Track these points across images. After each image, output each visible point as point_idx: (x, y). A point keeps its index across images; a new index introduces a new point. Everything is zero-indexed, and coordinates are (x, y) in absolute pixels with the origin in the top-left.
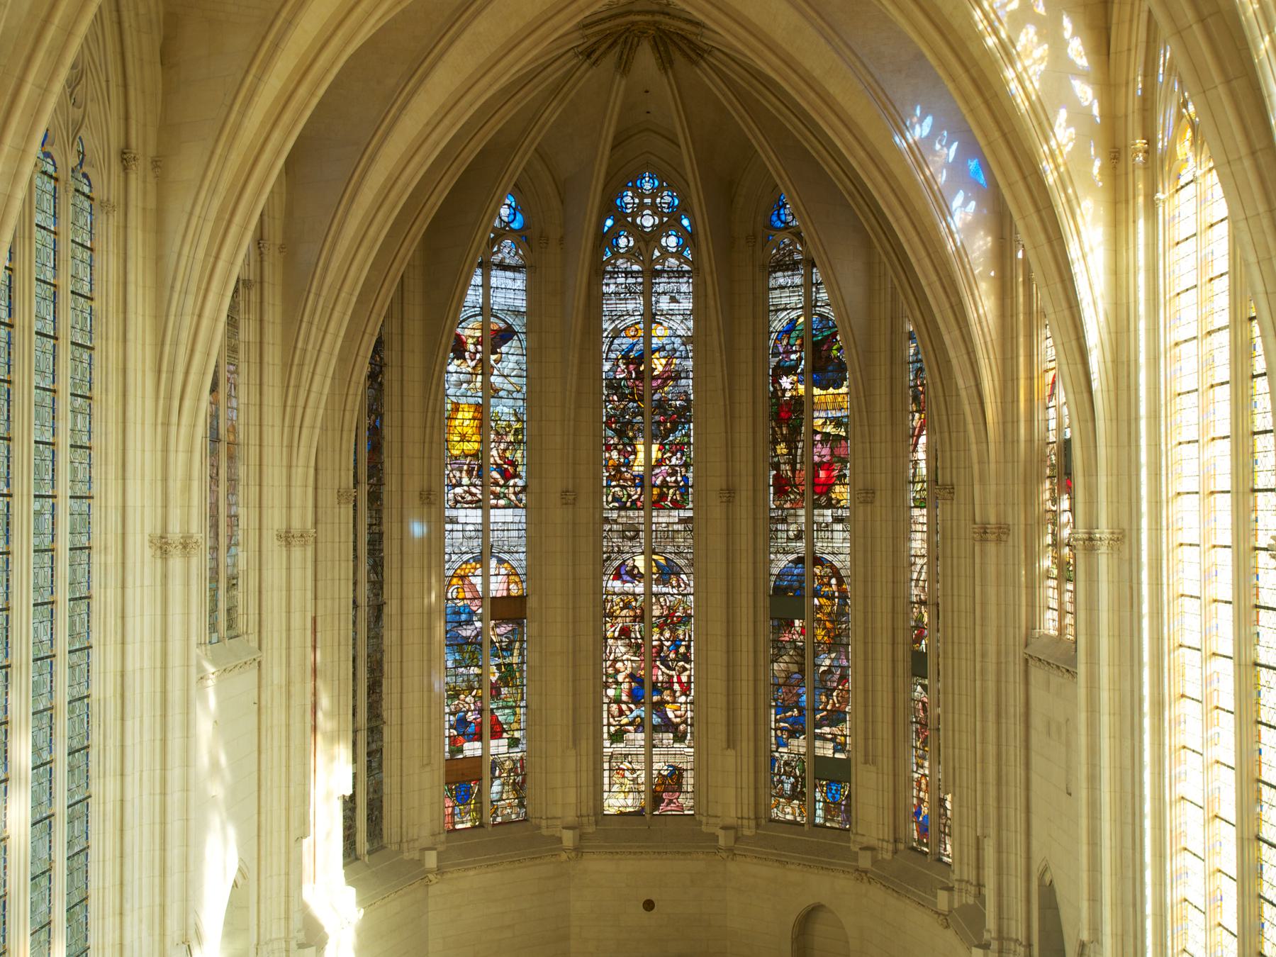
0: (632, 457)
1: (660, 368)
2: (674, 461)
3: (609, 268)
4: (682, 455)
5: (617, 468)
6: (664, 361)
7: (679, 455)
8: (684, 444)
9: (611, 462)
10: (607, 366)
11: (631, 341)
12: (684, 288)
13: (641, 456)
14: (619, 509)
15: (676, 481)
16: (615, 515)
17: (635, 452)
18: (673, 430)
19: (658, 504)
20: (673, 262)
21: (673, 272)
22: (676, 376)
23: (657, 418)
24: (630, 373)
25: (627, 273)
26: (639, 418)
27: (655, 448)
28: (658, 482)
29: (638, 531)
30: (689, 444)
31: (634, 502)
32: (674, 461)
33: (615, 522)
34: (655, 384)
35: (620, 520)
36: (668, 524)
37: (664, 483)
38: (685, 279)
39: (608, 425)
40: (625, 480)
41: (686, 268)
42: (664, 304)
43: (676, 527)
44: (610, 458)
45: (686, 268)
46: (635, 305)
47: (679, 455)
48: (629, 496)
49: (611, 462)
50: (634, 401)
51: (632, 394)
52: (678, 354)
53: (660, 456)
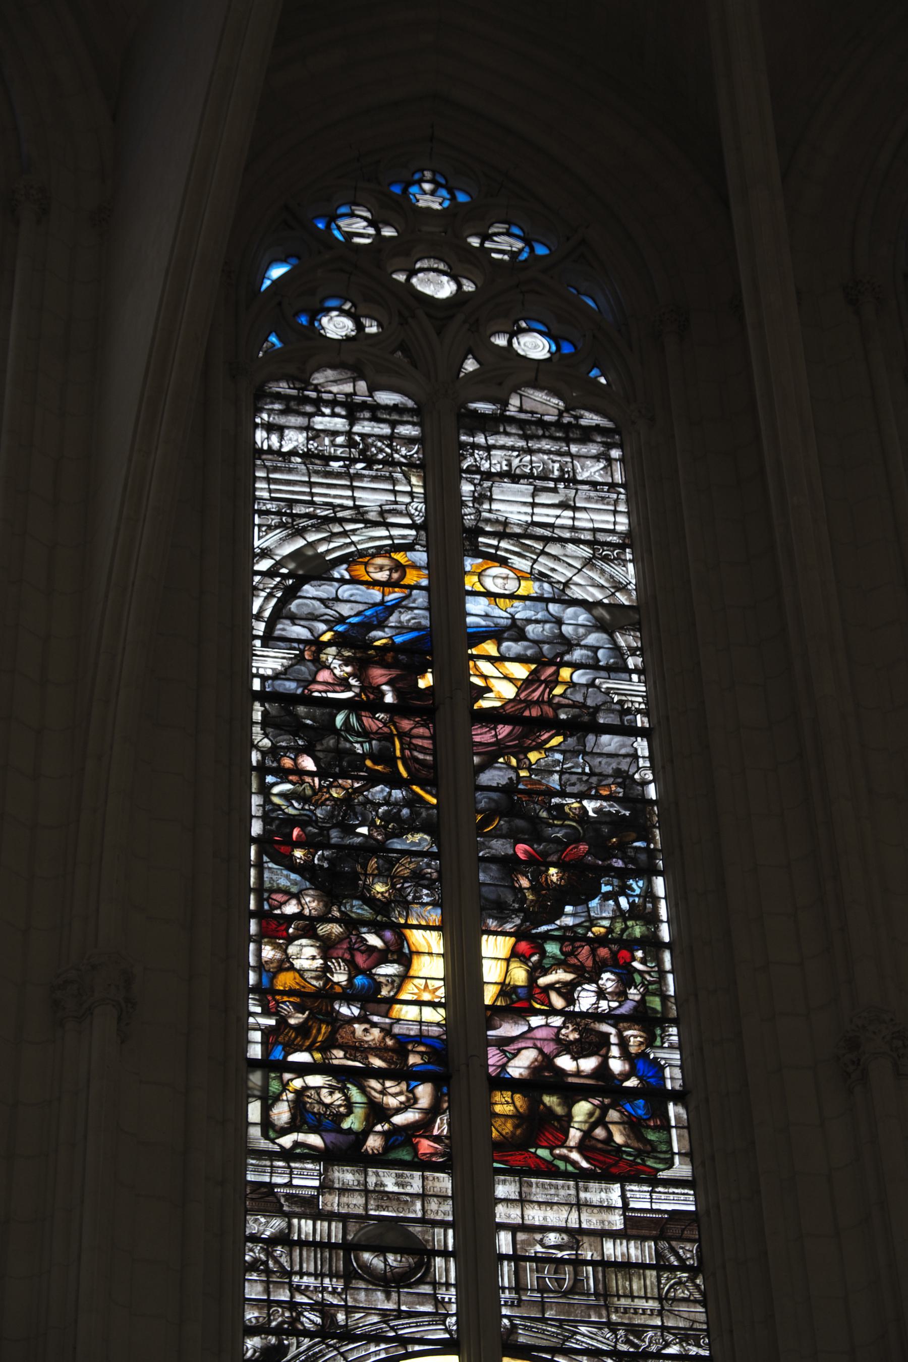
0: (389, 970)
1: (508, 691)
2: (586, 1000)
3: (283, 387)
4: (626, 978)
5: (318, 1000)
6: (520, 671)
7: (608, 980)
8: (632, 944)
9: (285, 980)
10: (268, 662)
11: (376, 595)
12: (592, 471)
13: (430, 968)
14: (328, 1157)
15: (603, 1069)
16: (306, 1179)
17: (404, 956)
18: (580, 888)
19: (529, 1148)
20: (544, 403)
21: (541, 423)
22: (583, 724)
23: (500, 847)
24: (368, 687)
25: (353, 410)
26: (418, 840)
27: (494, 948)
28: (518, 1068)
29: (423, 1254)
30: (653, 945)
31: (402, 1137)
32: (586, 1000)
33: (309, 1207)
34: (482, 736)
35: (331, 1202)
36: (576, 1235)
37: (545, 1077)
38: (593, 449)
39: (275, 846)
40: (356, 1049)
41: (590, 419)
42: (511, 505)
43: (612, 1250)
44: (285, 964)
45: (590, 419)
46: (392, 500)
47: (608, 980)
48: (377, 1112)
49: (285, 980)
50: (394, 781)
51: (385, 757)
52: (577, 655)
53: (519, 975)
